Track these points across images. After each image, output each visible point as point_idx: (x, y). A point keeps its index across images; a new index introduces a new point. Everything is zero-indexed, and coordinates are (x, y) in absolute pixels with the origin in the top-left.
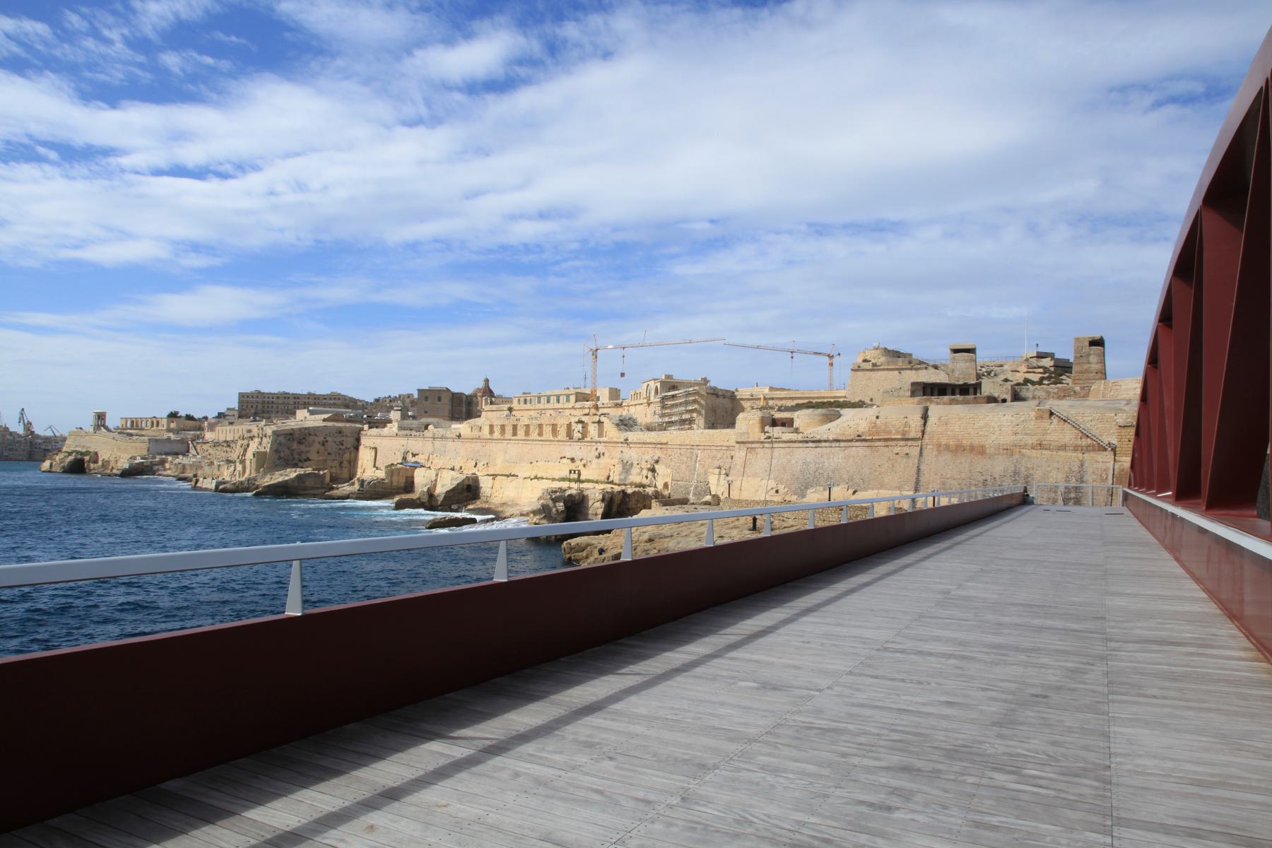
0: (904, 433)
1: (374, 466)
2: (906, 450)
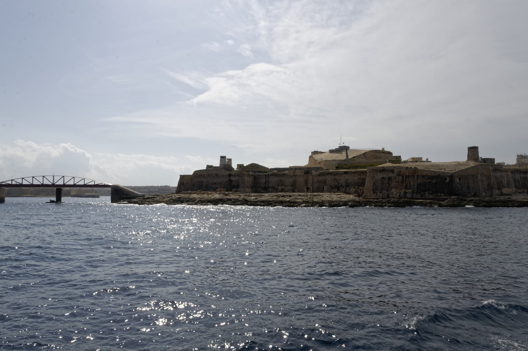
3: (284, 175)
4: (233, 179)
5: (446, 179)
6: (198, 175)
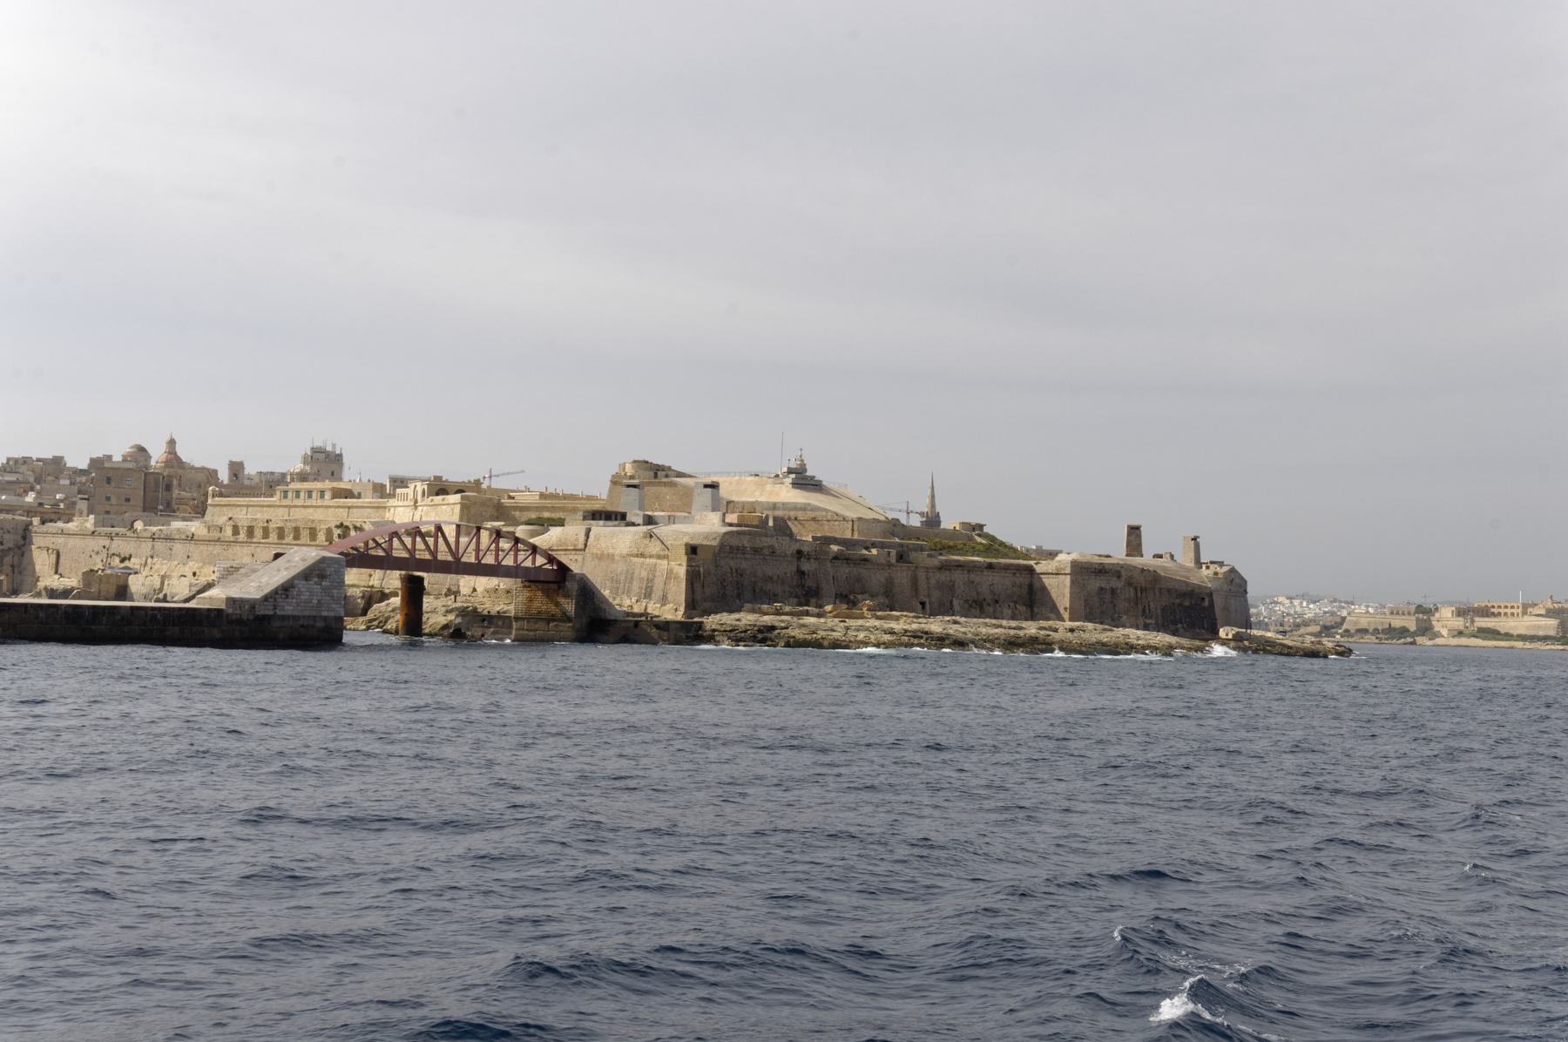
0: (575, 545)
1: (56, 572)
2: (576, 557)
3: (865, 560)
4: (806, 566)
5: (1203, 599)
6: (731, 547)
